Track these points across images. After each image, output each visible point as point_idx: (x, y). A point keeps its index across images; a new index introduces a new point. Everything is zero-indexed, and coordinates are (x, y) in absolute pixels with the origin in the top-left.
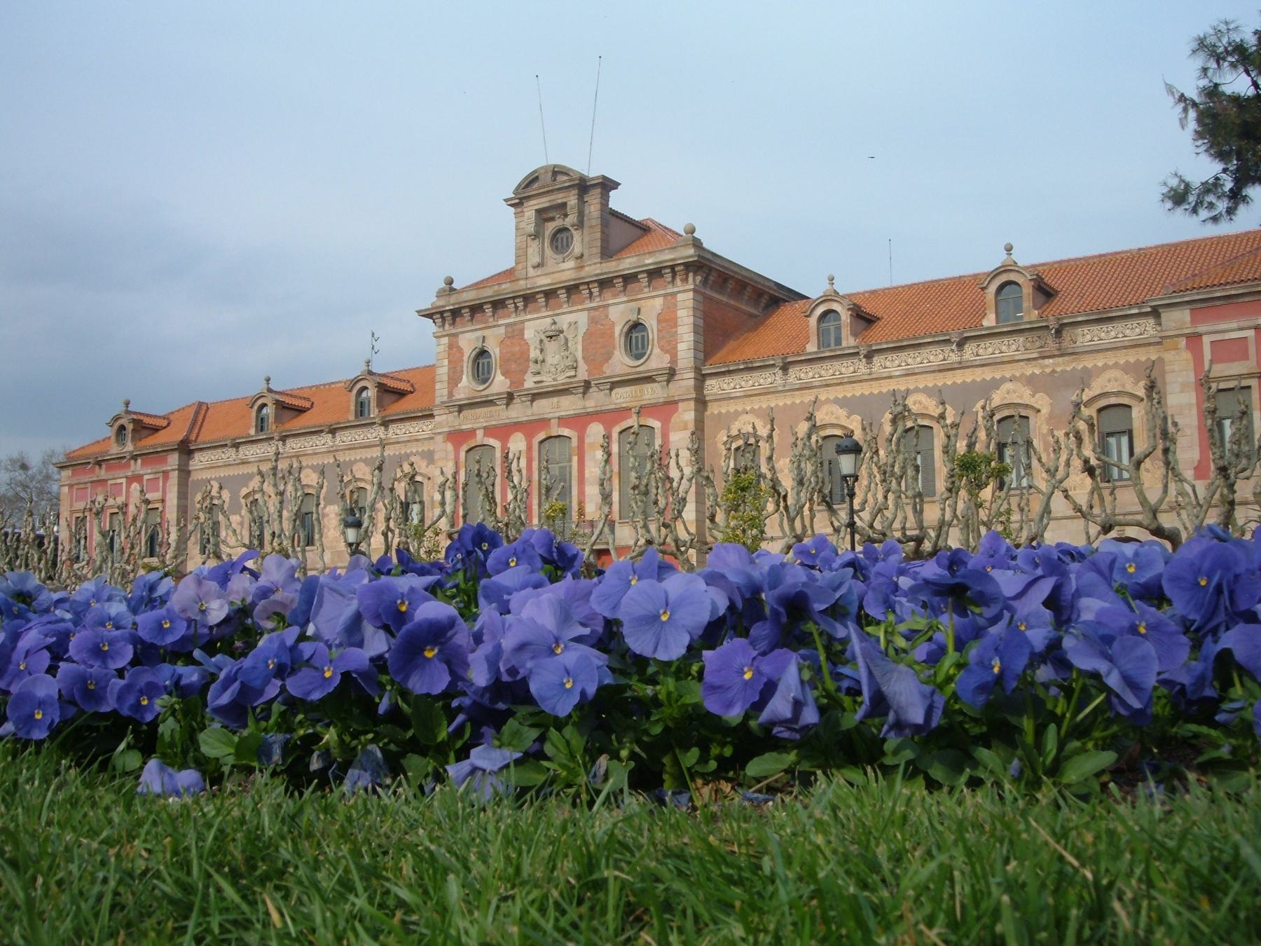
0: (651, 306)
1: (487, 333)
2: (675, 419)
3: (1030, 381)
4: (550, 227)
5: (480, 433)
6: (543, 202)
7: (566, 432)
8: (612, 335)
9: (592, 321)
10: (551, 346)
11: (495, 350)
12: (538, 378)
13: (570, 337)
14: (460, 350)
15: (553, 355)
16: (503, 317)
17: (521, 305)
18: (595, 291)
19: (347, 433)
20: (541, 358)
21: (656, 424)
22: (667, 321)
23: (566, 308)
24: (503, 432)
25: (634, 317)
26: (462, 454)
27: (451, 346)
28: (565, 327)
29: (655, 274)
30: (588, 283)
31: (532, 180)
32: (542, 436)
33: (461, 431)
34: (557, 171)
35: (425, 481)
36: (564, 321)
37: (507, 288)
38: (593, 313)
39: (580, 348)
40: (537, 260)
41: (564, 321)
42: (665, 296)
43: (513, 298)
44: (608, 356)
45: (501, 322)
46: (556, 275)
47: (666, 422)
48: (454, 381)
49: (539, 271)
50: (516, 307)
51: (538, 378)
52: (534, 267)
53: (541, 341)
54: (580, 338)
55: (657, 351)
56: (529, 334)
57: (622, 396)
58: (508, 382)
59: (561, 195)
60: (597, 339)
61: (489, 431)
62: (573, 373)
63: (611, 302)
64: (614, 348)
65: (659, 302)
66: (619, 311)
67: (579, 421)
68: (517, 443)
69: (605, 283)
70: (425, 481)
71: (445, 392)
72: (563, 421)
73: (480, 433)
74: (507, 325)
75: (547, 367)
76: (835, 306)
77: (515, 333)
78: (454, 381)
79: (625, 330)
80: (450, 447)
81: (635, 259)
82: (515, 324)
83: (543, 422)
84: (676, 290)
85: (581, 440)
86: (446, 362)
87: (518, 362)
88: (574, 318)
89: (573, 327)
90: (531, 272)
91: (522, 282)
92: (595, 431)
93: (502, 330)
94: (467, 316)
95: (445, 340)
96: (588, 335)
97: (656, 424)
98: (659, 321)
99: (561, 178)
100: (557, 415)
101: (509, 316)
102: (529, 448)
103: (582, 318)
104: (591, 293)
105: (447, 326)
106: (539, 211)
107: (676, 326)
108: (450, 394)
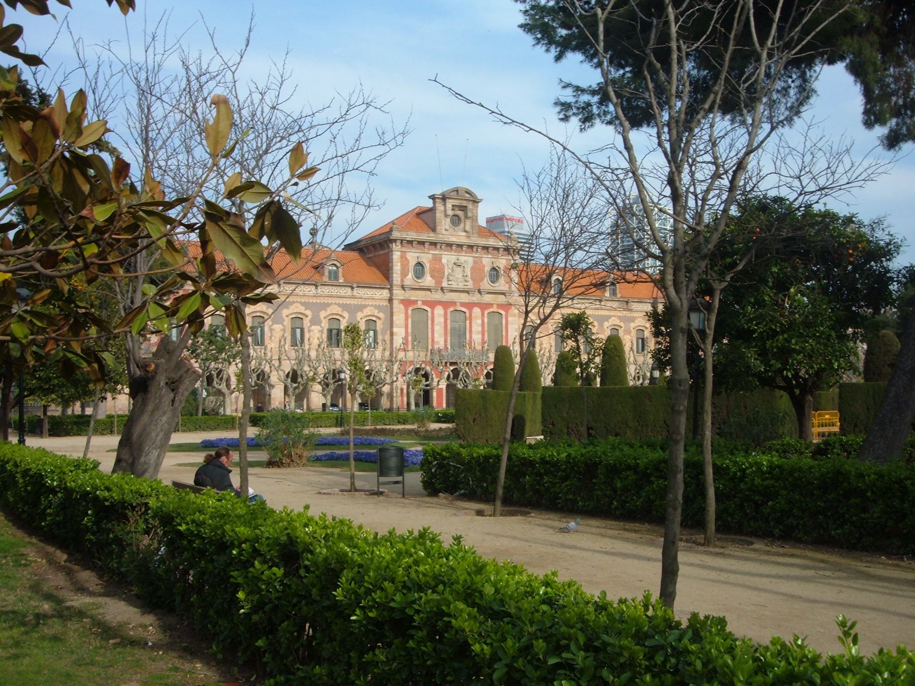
2: (510, 311)
3: (619, 318)
5: (420, 303)
6: (457, 202)
7: (464, 309)
9: (475, 262)
10: (459, 270)
15: (458, 273)
19: (326, 287)
21: (503, 313)
24: (433, 304)
26: (410, 312)
27: (402, 257)
31: (457, 191)
32: (452, 309)
33: (409, 300)
34: (468, 192)
35: (377, 320)
40: (447, 227)
44: (482, 280)
47: (507, 312)
48: (404, 274)
57: (488, 298)
61: (424, 303)
66: (487, 261)
67: (470, 306)
68: (439, 310)
70: (377, 320)
71: (399, 279)
72: (463, 304)
73: (420, 303)
77: (437, 259)
78: (404, 274)
80: (402, 307)
83: (453, 303)
85: (470, 314)
87: (438, 273)
88: (467, 259)
90: (444, 232)
92: (477, 311)
93: (430, 256)
96: (473, 269)
97: (503, 313)
102: (446, 314)
108: (402, 281)
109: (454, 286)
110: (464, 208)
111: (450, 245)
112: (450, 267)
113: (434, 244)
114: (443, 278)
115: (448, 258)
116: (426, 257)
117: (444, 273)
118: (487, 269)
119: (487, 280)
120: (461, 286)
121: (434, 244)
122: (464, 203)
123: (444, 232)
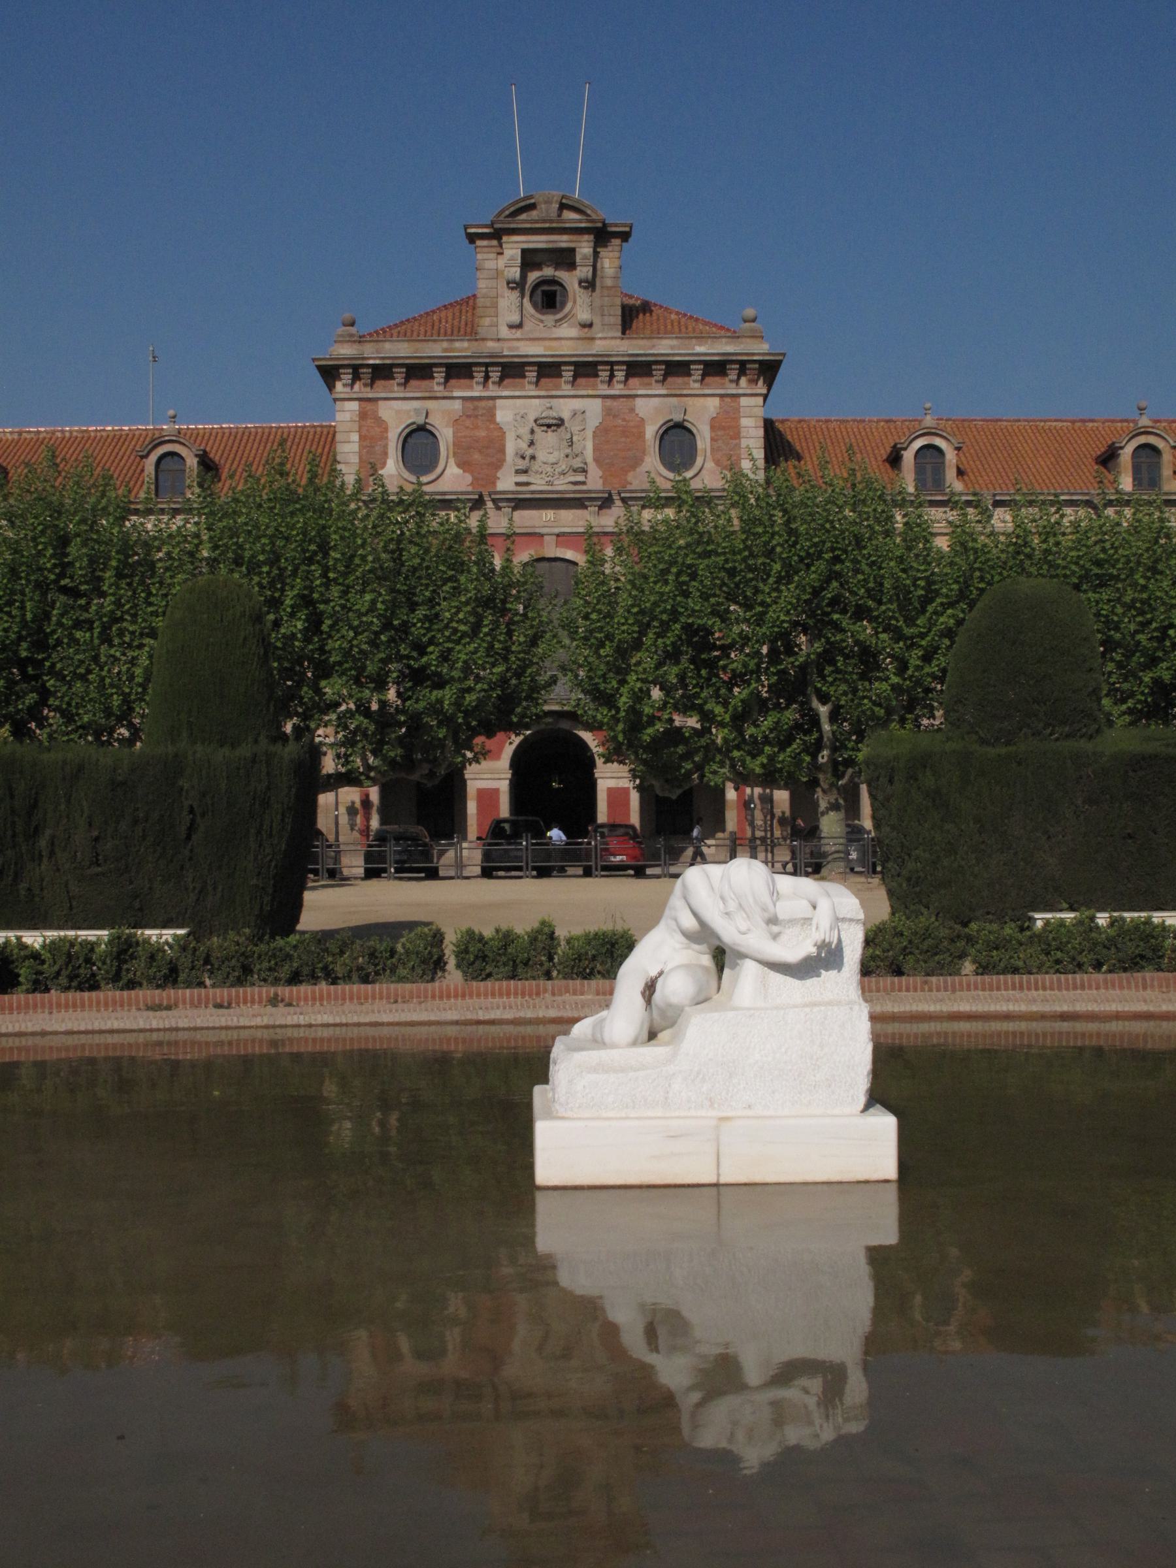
0: (702, 408)
1: (430, 404)
4: (533, 276)
7: (569, 555)
8: (641, 435)
9: (608, 413)
10: (547, 440)
11: (446, 435)
12: (523, 478)
13: (575, 429)
14: (383, 426)
15: (549, 447)
16: (460, 388)
17: (495, 375)
18: (620, 375)
20: (530, 452)
22: (724, 428)
23: (567, 389)
25: (678, 417)
27: (363, 415)
28: (566, 415)
29: (715, 368)
30: (612, 364)
36: (565, 408)
37: (462, 349)
38: (609, 402)
39: (589, 445)
40: (515, 318)
41: (565, 408)
42: (721, 396)
43: (487, 365)
44: (637, 462)
45: (455, 394)
46: (554, 344)
49: (518, 334)
50: (487, 377)
51: (523, 478)
52: (511, 327)
53: (532, 432)
54: (589, 434)
55: (710, 465)
56: (505, 413)
58: (469, 478)
59: (565, 237)
60: (617, 439)
62: (580, 478)
63: (640, 392)
64: (644, 452)
65: (713, 404)
66: (652, 406)
69: (638, 368)
72: (563, 538)
74: (464, 399)
75: (536, 466)
76: (938, 442)
77: (480, 413)
79: (661, 432)
81: (674, 342)
82: (480, 398)
84: (741, 391)
86: (355, 437)
87: (483, 451)
88: (583, 408)
89: (579, 417)
90: (504, 332)
91: (490, 344)
93: (457, 405)
94: (400, 378)
95: (354, 406)
96: (601, 432)
98: (713, 428)
99: (569, 215)
100: (557, 531)
101: (471, 388)
103: (594, 409)
104: (612, 376)
105: (357, 387)
106: (524, 252)
107: (737, 436)
109: (539, 484)
110: (566, 258)
111: (512, 370)
112: (524, 431)
113: (458, 371)
114: (499, 464)
115: (515, 410)
116: (444, 410)
117: (502, 450)
118: (651, 431)
119: (652, 462)
120: (562, 485)
121: (458, 371)
122: (563, 241)
123: (504, 332)
